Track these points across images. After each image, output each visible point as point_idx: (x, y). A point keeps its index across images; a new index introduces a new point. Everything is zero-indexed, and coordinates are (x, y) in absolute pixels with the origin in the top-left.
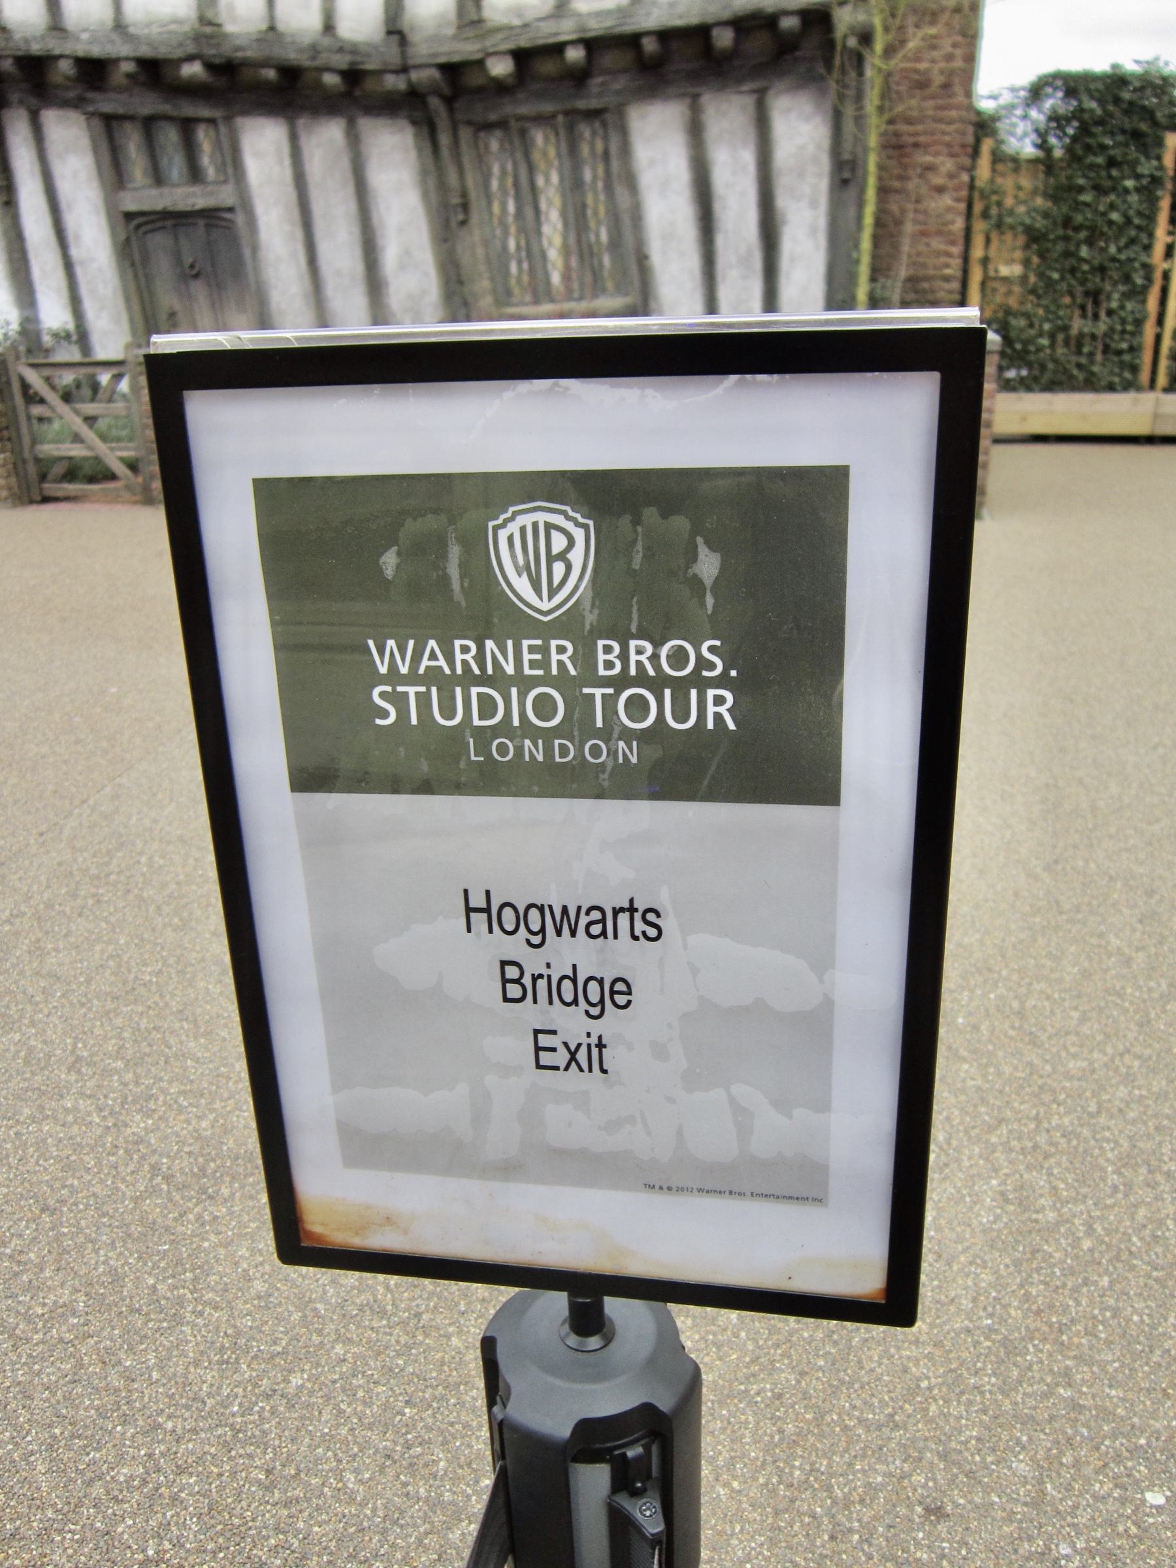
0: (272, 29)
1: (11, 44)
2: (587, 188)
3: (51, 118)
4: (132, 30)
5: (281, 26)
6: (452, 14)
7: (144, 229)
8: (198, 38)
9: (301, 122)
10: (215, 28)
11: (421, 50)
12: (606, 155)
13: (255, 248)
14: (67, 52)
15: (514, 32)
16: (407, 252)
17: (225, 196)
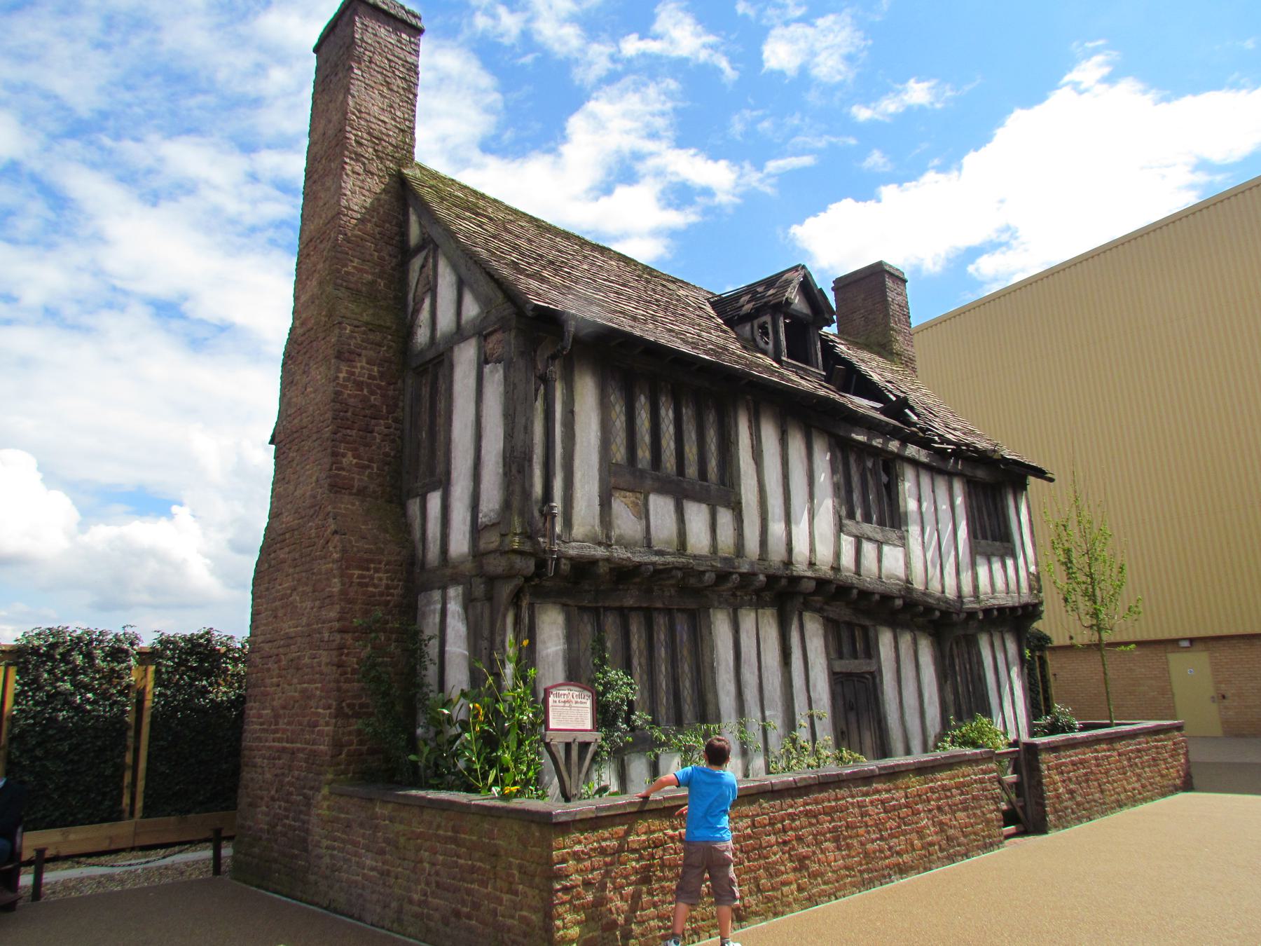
16: (931, 697)
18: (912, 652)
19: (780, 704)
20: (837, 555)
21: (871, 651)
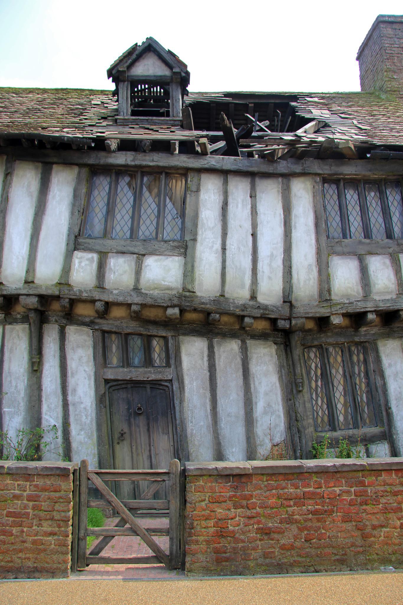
0: (222, 296)
1: (71, 292)
2: (356, 376)
3: (71, 331)
4: (143, 291)
5: (227, 295)
6: (316, 296)
7: (113, 388)
8: (180, 297)
9: (215, 340)
10: (191, 294)
11: (300, 310)
12: (365, 361)
13: (181, 401)
14: (102, 298)
15: (345, 305)
16: (269, 405)
17: (169, 374)
18: (239, 361)
19: (22, 404)
20: (67, 269)
21: (172, 358)
